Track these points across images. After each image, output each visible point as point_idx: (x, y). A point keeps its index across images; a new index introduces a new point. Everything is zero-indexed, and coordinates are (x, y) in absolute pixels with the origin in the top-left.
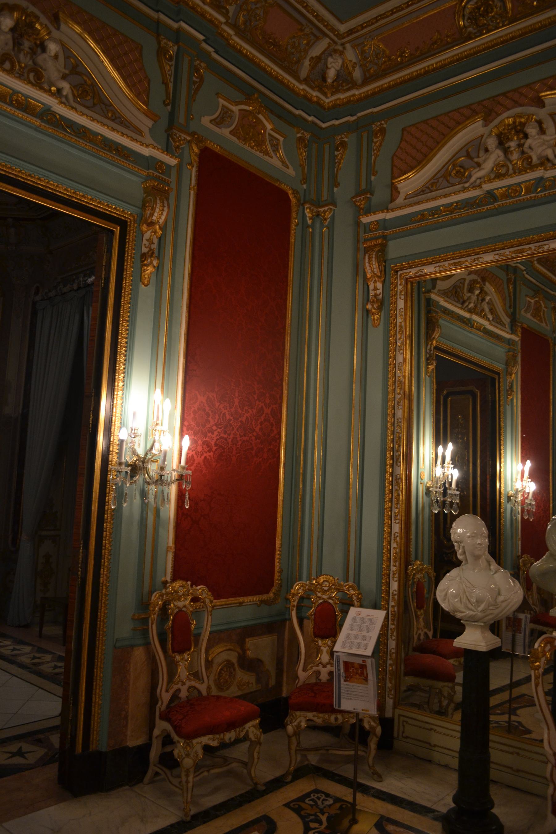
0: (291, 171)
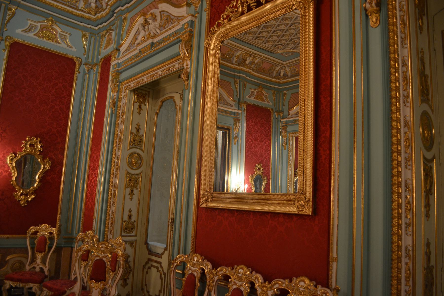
0: (74, 49)
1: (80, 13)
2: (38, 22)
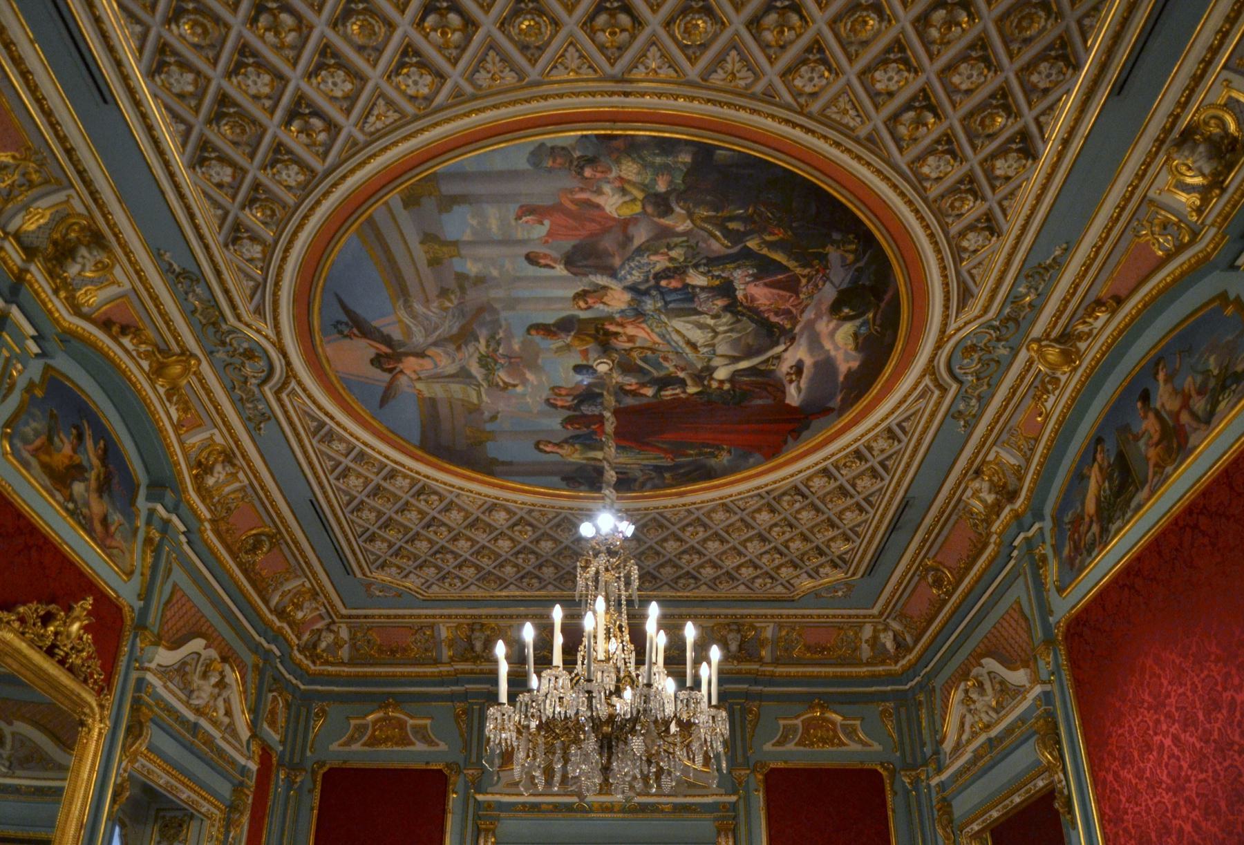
0: (877, 747)
2: (796, 717)
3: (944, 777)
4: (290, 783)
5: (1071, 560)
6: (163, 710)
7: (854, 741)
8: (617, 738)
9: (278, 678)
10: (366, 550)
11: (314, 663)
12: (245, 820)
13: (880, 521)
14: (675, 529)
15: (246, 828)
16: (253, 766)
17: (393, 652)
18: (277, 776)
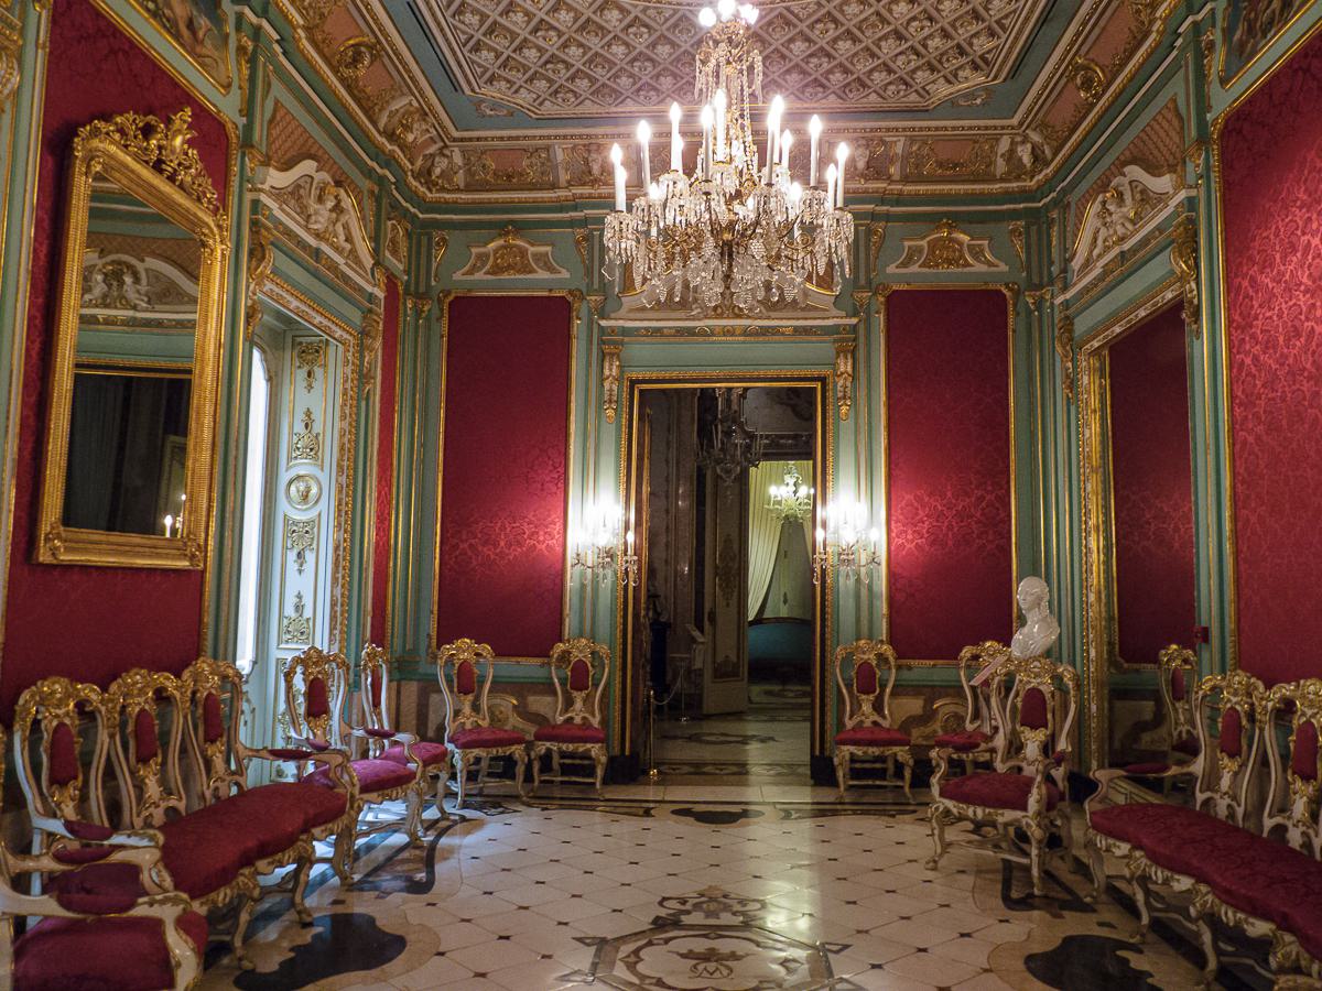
0: (1003, 268)
1: (997, 186)
3: (1068, 295)
4: (418, 313)
5: (1242, 45)
6: (283, 233)
7: (980, 261)
8: (738, 244)
9: (395, 206)
10: (473, 62)
11: (431, 191)
12: (378, 344)
13: (1031, 11)
14: (803, 26)
15: (380, 354)
16: (381, 294)
17: (509, 177)
18: (405, 304)
